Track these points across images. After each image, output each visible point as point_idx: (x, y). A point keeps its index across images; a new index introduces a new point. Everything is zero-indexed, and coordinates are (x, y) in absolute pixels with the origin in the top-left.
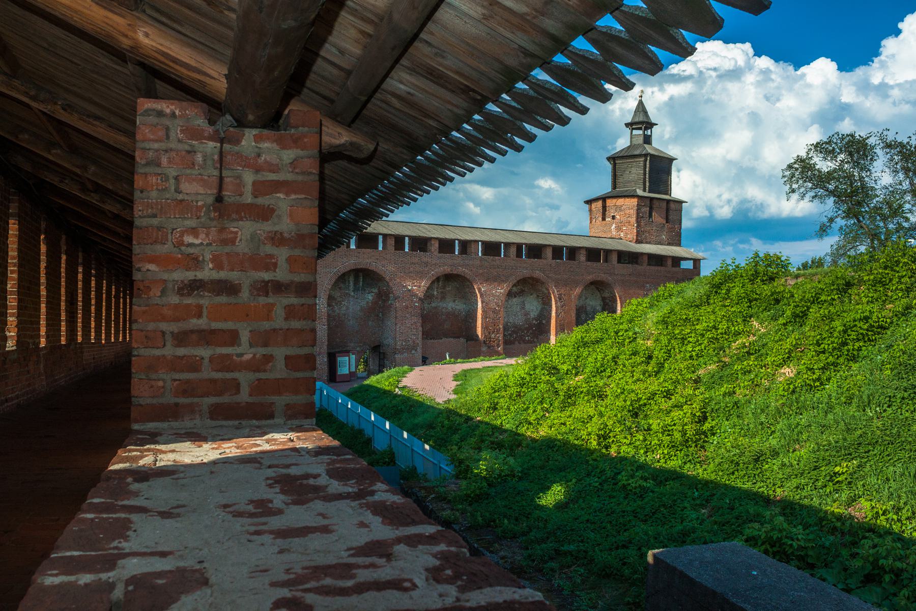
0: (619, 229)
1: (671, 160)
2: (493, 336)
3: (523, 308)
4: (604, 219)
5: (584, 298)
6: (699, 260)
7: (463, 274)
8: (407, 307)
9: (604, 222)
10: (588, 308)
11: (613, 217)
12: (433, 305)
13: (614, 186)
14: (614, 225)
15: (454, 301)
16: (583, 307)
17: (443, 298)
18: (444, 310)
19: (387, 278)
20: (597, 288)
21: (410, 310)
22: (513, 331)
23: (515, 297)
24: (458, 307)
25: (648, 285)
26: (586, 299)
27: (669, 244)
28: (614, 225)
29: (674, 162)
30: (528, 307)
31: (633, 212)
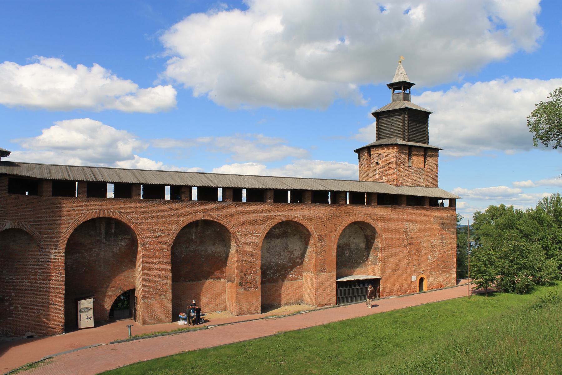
0: (381, 173)
1: (427, 114)
2: (250, 278)
3: (286, 248)
4: (369, 166)
5: (347, 236)
6: (455, 199)
7: (216, 220)
8: (155, 254)
9: (369, 168)
10: (352, 246)
11: (377, 163)
12: (192, 249)
13: (379, 138)
14: (377, 171)
15: (214, 244)
16: (346, 245)
17: (202, 242)
18: (202, 253)
19: (133, 227)
20: (361, 228)
21: (158, 256)
22: (276, 270)
23: (278, 238)
24: (218, 250)
25: (407, 223)
26: (350, 237)
27: (427, 186)
28: (377, 171)
29: (430, 116)
30: (291, 247)
31: (393, 158)
